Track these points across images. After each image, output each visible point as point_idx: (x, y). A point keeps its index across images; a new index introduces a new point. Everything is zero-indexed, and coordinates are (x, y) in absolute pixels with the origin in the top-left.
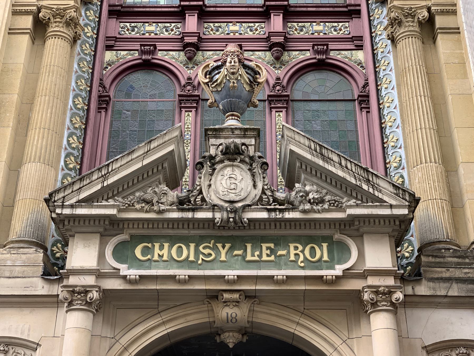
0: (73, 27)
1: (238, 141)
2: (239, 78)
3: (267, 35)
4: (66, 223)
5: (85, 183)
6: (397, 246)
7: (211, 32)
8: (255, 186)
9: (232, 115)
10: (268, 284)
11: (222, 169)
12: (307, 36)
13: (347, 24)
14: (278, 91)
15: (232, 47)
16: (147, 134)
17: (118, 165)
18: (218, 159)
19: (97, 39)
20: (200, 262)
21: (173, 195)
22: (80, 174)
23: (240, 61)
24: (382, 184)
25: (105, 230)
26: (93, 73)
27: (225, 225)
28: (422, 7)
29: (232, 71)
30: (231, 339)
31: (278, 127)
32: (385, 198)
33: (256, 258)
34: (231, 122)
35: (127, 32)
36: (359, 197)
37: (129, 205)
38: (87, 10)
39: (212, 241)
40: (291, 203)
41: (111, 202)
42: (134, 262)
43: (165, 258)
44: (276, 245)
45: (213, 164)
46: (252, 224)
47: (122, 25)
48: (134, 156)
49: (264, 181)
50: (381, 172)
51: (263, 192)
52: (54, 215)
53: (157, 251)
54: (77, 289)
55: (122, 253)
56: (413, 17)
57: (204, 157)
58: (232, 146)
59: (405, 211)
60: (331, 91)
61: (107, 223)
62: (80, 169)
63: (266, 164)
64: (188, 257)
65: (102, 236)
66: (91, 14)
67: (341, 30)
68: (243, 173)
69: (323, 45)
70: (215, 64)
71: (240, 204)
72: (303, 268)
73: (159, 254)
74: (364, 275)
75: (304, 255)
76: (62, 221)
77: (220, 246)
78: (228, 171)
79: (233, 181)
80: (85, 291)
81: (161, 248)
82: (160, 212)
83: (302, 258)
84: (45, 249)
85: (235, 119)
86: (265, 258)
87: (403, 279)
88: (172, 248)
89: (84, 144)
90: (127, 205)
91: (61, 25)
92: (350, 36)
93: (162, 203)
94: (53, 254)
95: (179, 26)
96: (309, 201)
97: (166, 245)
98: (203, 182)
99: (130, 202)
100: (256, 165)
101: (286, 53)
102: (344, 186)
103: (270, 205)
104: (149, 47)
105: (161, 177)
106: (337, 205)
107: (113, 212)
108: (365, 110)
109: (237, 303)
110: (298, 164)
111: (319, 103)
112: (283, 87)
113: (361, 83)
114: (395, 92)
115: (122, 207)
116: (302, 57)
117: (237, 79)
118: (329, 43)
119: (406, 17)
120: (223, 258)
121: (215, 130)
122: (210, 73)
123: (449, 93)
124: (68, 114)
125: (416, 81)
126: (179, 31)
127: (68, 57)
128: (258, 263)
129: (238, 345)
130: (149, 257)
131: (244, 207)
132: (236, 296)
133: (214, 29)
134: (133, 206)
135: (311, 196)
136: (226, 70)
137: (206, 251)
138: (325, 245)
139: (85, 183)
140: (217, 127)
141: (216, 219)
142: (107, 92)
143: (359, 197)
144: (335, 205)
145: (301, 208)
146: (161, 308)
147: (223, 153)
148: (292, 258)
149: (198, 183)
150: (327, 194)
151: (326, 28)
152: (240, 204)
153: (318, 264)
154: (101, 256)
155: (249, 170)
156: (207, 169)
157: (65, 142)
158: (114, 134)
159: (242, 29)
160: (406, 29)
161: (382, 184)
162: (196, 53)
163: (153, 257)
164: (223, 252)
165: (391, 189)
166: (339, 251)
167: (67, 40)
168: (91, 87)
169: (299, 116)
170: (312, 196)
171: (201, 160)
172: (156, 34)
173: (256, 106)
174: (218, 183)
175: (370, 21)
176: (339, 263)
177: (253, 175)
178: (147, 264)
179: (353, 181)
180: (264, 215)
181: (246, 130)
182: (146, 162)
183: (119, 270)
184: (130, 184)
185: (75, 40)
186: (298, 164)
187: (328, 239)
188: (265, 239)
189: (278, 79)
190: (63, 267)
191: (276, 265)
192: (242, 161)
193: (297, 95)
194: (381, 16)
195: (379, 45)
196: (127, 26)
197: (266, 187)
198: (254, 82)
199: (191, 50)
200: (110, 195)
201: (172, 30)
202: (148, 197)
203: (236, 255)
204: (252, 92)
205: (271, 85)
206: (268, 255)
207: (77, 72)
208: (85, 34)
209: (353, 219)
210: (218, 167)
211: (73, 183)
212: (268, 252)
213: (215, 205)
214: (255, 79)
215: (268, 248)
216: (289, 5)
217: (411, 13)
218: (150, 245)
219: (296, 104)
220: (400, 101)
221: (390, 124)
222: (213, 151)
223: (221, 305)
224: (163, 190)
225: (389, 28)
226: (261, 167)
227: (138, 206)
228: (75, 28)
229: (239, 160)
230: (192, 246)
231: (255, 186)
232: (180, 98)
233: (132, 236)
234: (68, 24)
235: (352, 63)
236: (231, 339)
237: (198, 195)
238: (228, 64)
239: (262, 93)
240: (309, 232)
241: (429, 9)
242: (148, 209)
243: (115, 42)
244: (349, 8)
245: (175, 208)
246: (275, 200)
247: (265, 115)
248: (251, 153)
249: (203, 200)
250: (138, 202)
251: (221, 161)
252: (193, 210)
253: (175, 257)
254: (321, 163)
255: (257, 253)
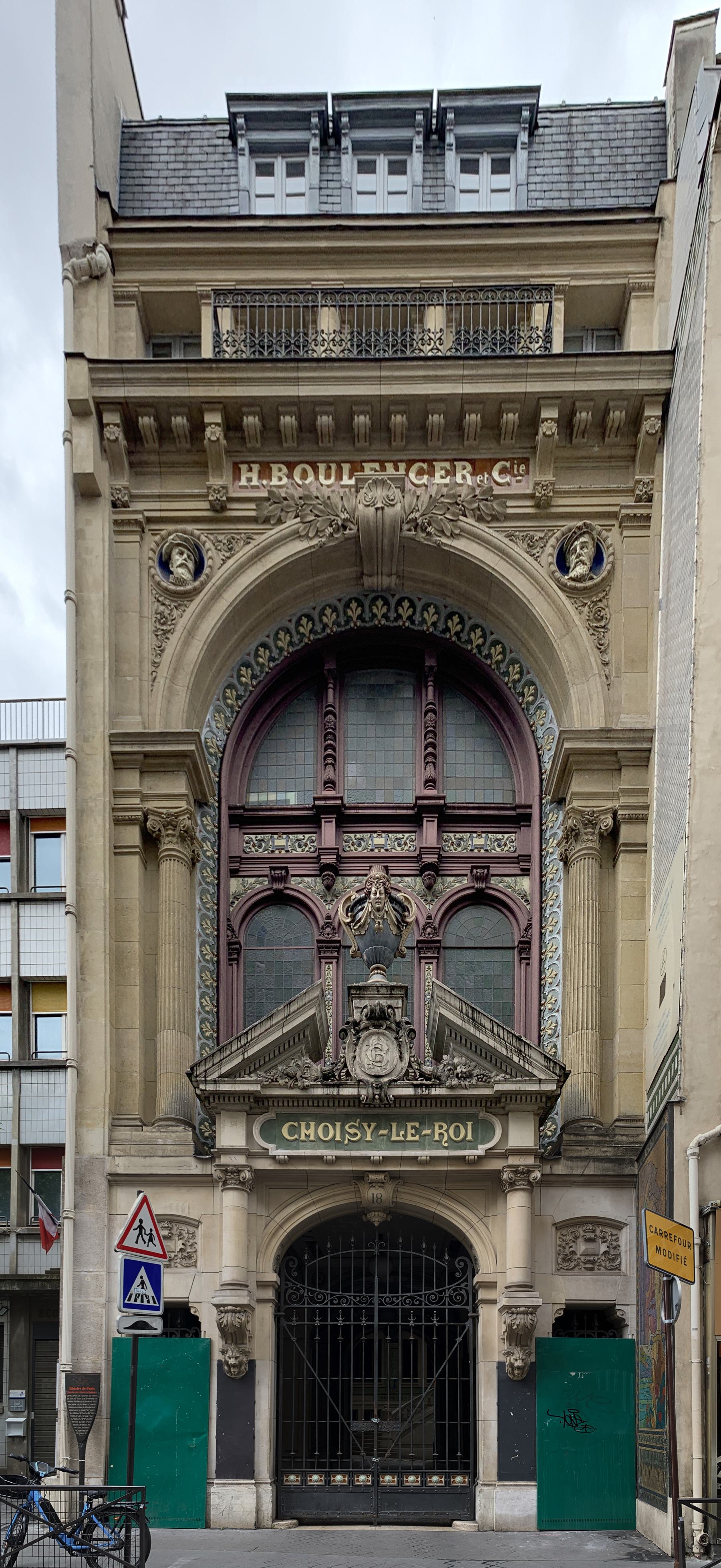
1: (384, 1002)
3: (418, 852)
4: (211, 1100)
5: (225, 1054)
6: (540, 1125)
8: (401, 1058)
9: (378, 968)
10: (411, 1166)
12: (465, 853)
13: (513, 836)
15: (377, 871)
16: (286, 995)
17: (257, 1033)
19: (219, 859)
21: (317, 1069)
22: (218, 1044)
23: (386, 892)
24: (534, 1055)
26: (218, 910)
27: (370, 1103)
30: (376, 1218)
34: (376, 978)
36: (509, 1071)
38: (203, 815)
40: (438, 1078)
42: (282, 1143)
43: (312, 1138)
45: (358, 1032)
46: (398, 1101)
47: (246, 837)
48: (275, 1021)
50: (533, 1042)
51: (410, 1066)
52: (198, 1092)
54: (229, 1168)
55: (270, 1132)
57: (348, 1023)
58: (378, 1009)
59: (553, 1087)
60: (488, 936)
62: (218, 1038)
63: (413, 1031)
68: (389, 1042)
69: (483, 868)
70: (358, 896)
71: (386, 1079)
72: (446, 1148)
74: (505, 1155)
76: (207, 1098)
78: (373, 1040)
79: (379, 1052)
80: (238, 1170)
82: (305, 1088)
84: (194, 1128)
87: (542, 1159)
89: (218, 1006)
91: (175, 840)
92: (516, 855)
94: (202, 1134)
96: (457, 1076)
98: (347, 1054)
100: (402, 1032)
102: (494, 1058)
105: (303, 1047)
108: (524, 962)
109: (382, 1184)
110: (447, 1032)
111: (474, 951)
112: (435, 929)
113: (524, 923)
114: (560, 938)
117: (382, 918)
119: (585, 825)
120: (369, 1138)
121: (359, 988)
122: (353, 908)
124: (197, 969)
125: (584, 921)
127: (188, 888)
128: (403, 1144)
129: (383, 1224)
131: (391, 1082)
132: (381, 1177)
135: (459, 1070)
138: (470, 1124)
139: (225, 1054)
140: (360, 984)
143: (509, 1071)
146: (310, 1189)
147: (369, 1018)
152: (386, 1079)
153: (461, 1144)
154: (249, 1136)
155: (396, 1038)
156: (351, 1038)
157: (198, 1005)
158: (249, 994)
161: (534, 1055)
165: (543, 1061)
166: (483, 1130)
168: (218, 930)
169: (451, 969)
171: (344, 1027)
172: (287, 851)
173: (403, 956)
174: (363, 1054)
175: (541, 830)
176: (483, 1143)
177: (400, 1046)
178: (294, 1144)
179: (504, 1052)
180: (410, 1091)
181: (393, 988)
182: (286, 1029)
184: (272, 1056)
186: (447, 1032)
187: (473, 1118)
189: (429, 917)
190: (213, 1147)
191: (420, 1145)
192: (388, 1028)
193: (450, 941)
194: (556, 823)
195: (549, 870)
198: (402, 923)
202: (291, 1071)
204: (399, 936)
205: (421, 927)
206: (413, 1135)
209: (500, 1097)
210: (363, 1035)
211: (213, 1054)
213: (360, 1081)
214: (403, 917)
220: (565, 950)
221: (550, 980)
222: (357, 1016)
223: (367, 1186)
230: (338, 1124)
231: (401, 1058)
235: (515, 895)
236: (376, 1218)
239: (411, 938)
240: (455, 1109)
241: (615, 814)
244: (520, 811)
246: (422, 1074)
247: (413, 968)
248: (398, 1019)
249: (348, 1074)
254: (472, 1030)
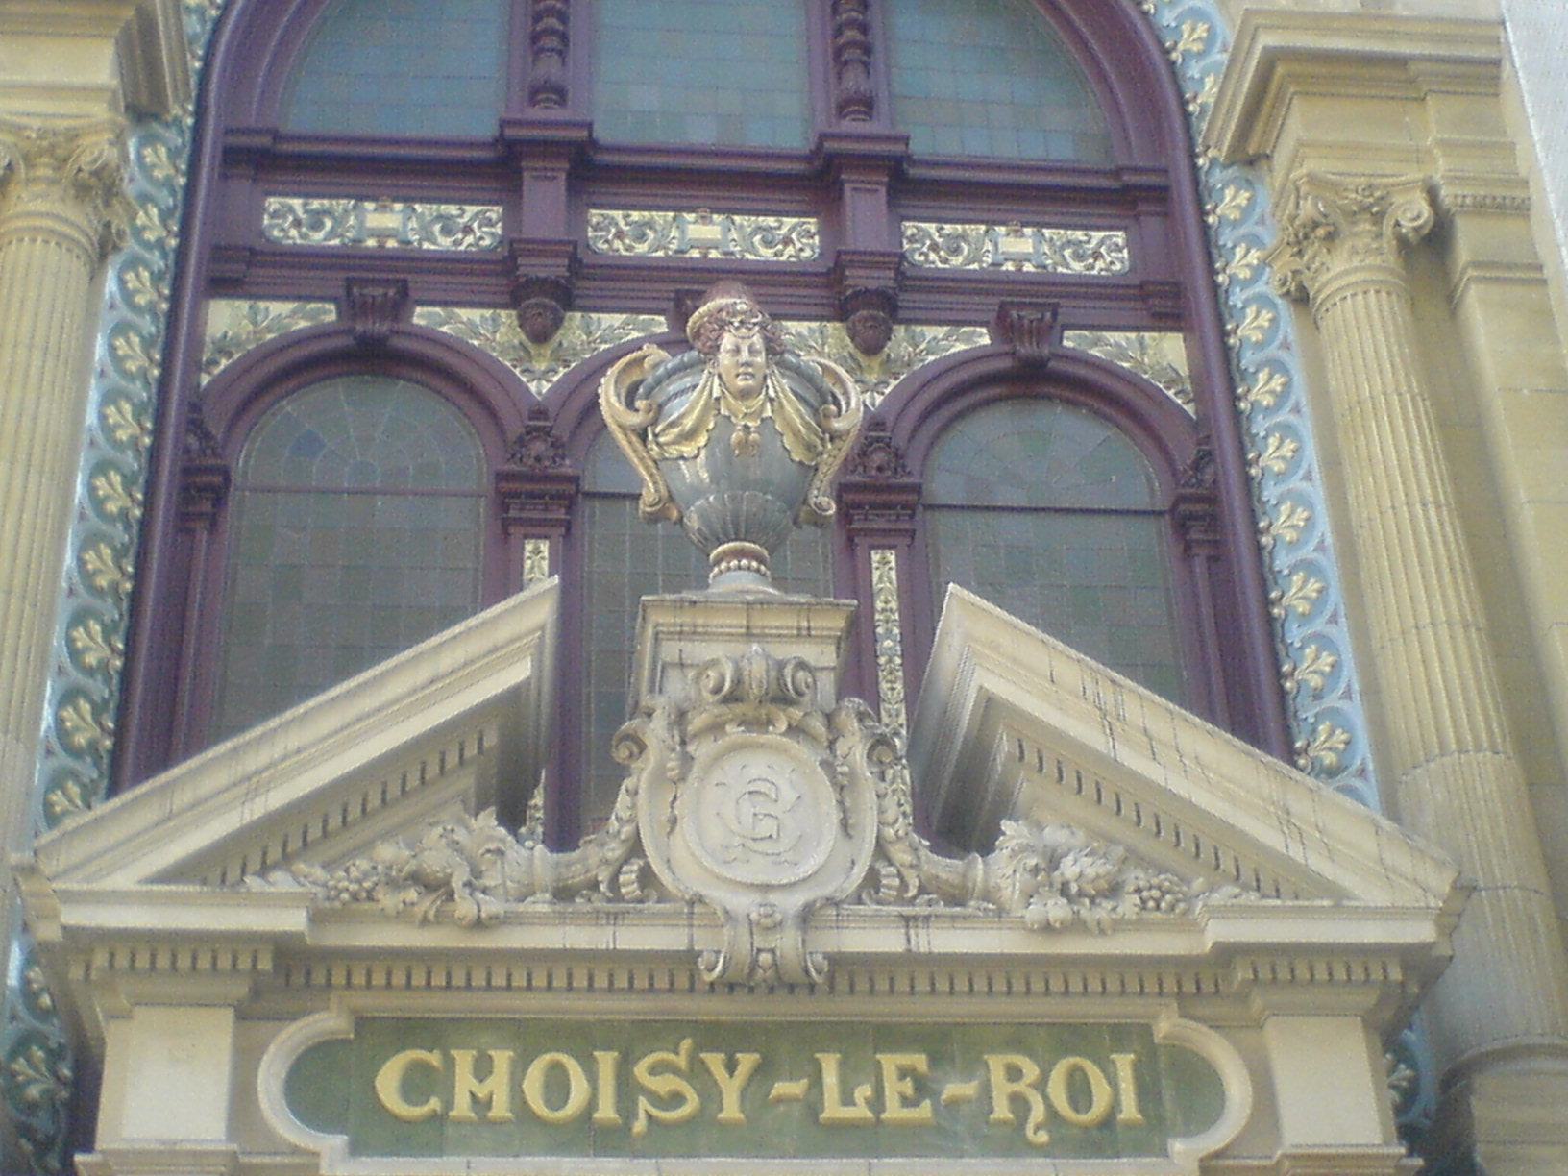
0: (99, 201)
2: (768, 413)
7: (617, 244)
9: (739, 554)
11: (718, 758)
14: (880, 469)
18: (697, 722)
20: (640, 1125)
25: (256, 993)
28: (1406, 187)
29: (740, 383)
31: (879, 605)
32: (1347, 880)
33: (861, 1112)
35: (293, 232)
37: (355, 897)
39: (686, 1044)
41: (281, 881)
44: (934, 1061)
49: (881, 811)
51: (881, 850)
53: (465, 1083)
56: (1378, 218)
61: (265, 964)
64: (592, 1105)
65: (242, 1015)
66: (157, 156)
67: (1097, 255)
73: (472, 1095)
75: (1046, 1098)
77: (715, 1061)
81: (483, 1069)
82: (479, 924)
83: (1038, 1112)
85: (749, 568)
86: (894, 1111)
88: (525, 1069)
90: (345, 896)
93: (484, 891)
95: (494, 216)
96: (1064, 891)
97: (502, 1059)
99: (359, 882)
101: (902, 328)
103: (912, 902)
104: (381, 291)
106: (1172, 908)
107: (293, 921)
115: (327, 905)
116: (960, 347)
118: (1062, 302)
123: (1523, 495)
126: (492, 234)
130: (434, 1104)
133: (624, 231)
134: (370, 898)
136: (716, 381)
137: (663, 1084)
141: (700, 954)
142: (215, 454)
144: (1163, 905)
145: (1034, 912)
148: (1002, 1111)
149: (625, 815)
150: (1125, 860)
151: (1046, 248)
159: (734, 234)
160: (1356, 263)
162: (562, 320)
163: (449, 1103)
164: (731, 1089)
167: (76, 251)
170: (1077, 869)
180: (888, 941)
183: (316, 1154)
185: (105, 247)
188: (890, 1036)
196: (291, 210)
197: (890, 832)
199: (545, 307)
200: (274, 854)
201: (467, 230)
203: (780, 1100)
207: (102, 373)
208: (137, 232)
209: (1227, 954)
212: (908, 1087)
213: (698, 900)
215: (904, 1073)
216: (907, 158)
217: (1372, 205)
218: (434, 1058)
219: (943, 522)
224: (490, 838)
225: (1286, 257)
226: (869, 757)
227: (388, 901)
228: (107, 204)
229: (783, 728)
232: (506, 486)
233: (363, 1023)
234: (82, 190)
237: (626, 861)
238: (724, 358)
242: (431, 914)
243: (249, 264)
245: (545, 908)
249: (647, 877)
250: (394, 884)
251: (716, 728)
252: (615, 918)
253: (538, 1106)
255: (863, 1091)
